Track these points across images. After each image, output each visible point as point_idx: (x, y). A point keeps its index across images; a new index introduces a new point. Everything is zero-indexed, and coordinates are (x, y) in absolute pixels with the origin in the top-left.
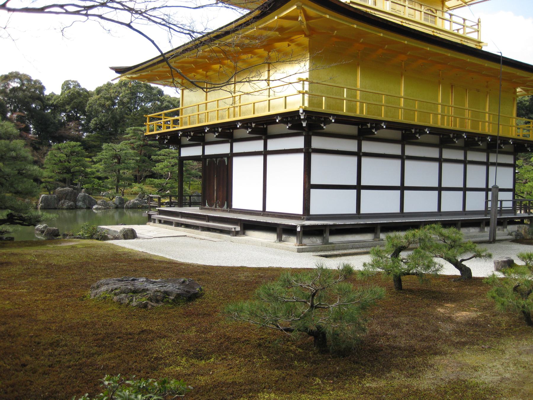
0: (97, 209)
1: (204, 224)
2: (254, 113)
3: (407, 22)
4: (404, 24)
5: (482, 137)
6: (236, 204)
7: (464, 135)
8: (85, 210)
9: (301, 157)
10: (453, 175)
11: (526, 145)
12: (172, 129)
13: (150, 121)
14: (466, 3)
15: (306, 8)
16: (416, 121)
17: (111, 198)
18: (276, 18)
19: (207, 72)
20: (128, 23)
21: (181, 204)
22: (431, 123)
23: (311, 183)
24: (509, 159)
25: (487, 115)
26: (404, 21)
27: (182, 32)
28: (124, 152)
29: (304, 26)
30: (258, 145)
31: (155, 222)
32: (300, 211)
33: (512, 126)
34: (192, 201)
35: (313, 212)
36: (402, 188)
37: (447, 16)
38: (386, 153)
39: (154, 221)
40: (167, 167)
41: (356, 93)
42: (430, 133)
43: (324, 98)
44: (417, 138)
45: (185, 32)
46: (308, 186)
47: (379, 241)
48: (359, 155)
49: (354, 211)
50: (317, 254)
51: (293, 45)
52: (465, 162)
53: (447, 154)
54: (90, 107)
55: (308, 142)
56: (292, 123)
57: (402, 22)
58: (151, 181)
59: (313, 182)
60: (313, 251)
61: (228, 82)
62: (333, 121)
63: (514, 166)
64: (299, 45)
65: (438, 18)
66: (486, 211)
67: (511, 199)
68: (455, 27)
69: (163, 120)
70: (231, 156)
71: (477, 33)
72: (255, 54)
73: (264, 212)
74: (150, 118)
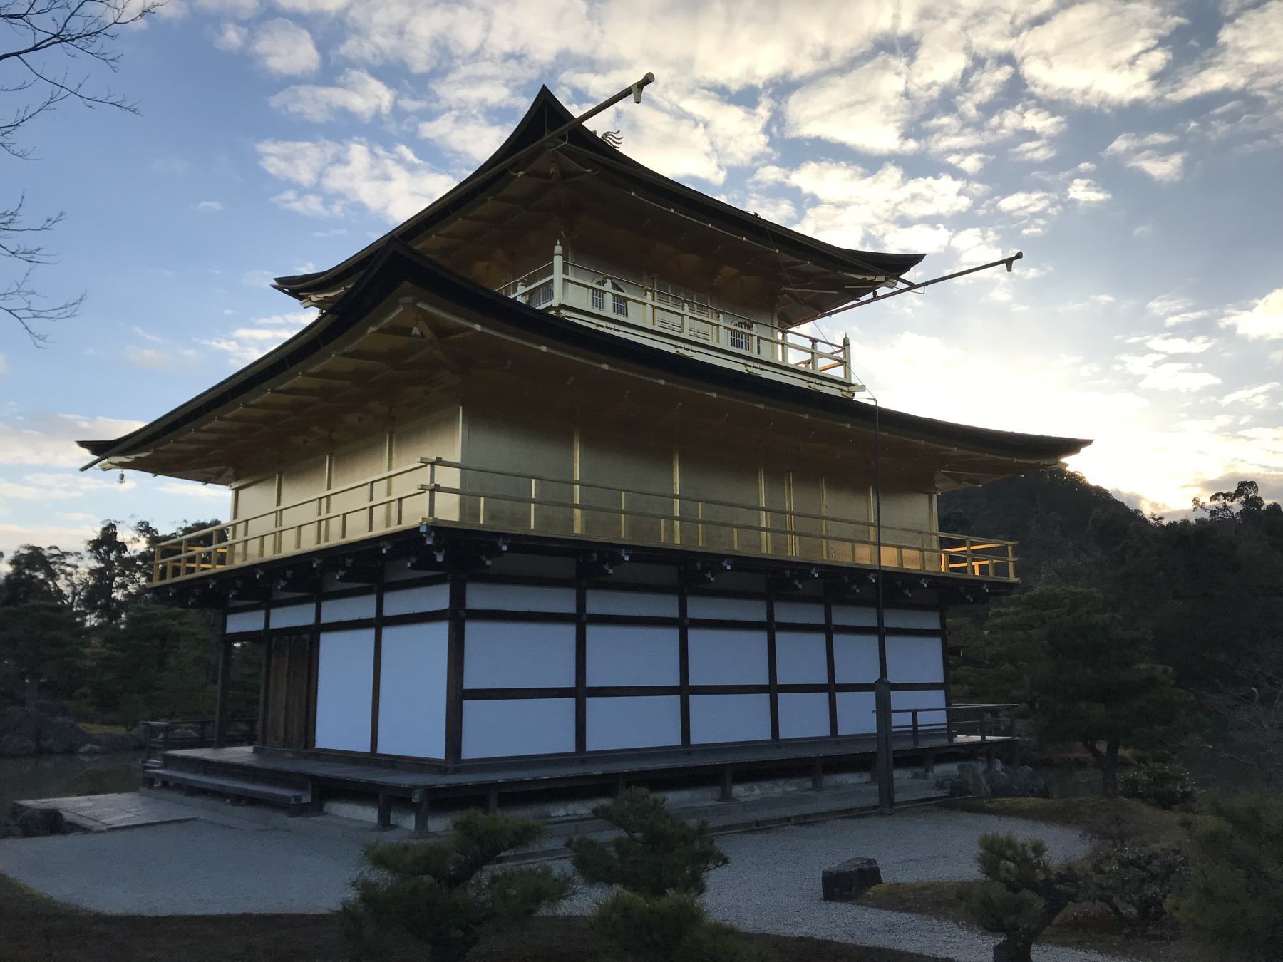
3: (688, 346)
4: (682, 351)
9: (441, 631)
10: (801, 657)
11: (962, 589)
13: (162, 557)
16: (701, 544)
23: (466, 687)
24: (933, 622)
30: (364, 607)
39: (149, 782)
46: (458, 695)
48: (581, 620)
49: (569, 746)
52: (828, 630)
53: (784, 613)
55: (458, 597)
59: (469, 684)
62: (505, 548)
70: (320, 628)
73: (373, 759)
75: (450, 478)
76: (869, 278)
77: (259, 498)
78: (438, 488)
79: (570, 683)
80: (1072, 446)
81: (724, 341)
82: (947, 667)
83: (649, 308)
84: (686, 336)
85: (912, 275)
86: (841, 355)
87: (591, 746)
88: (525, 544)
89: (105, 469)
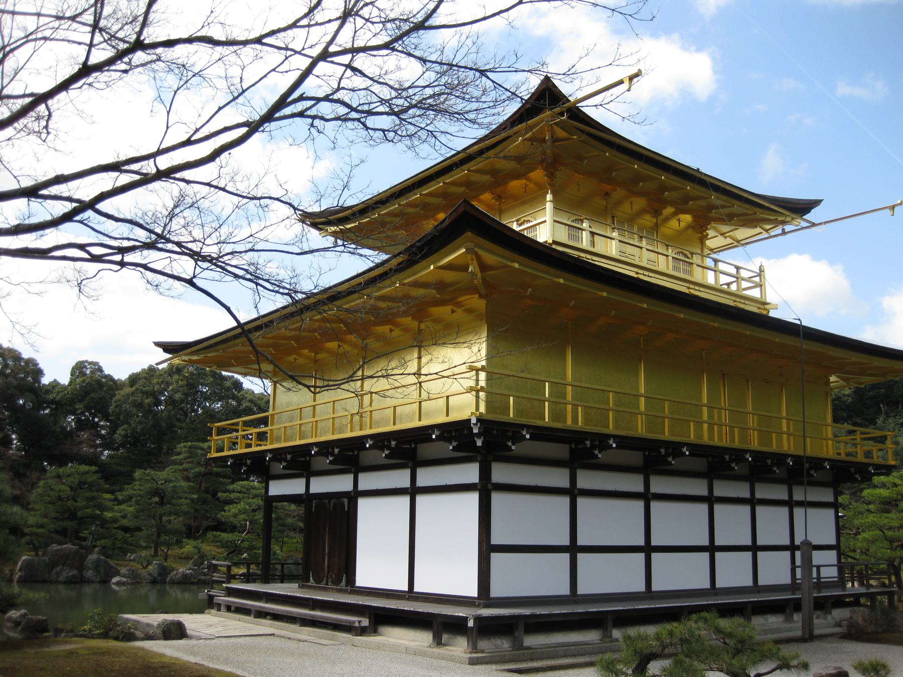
0: (118, 584)
1: (306, 615)
2: (394, 424)
4: (641, 277)
5: (779, 459)
7: (748, 456)
8: (98, 585)
9: (473, 498)
10: (733, 524)
11: (852, 470)
12: (254, 449)
14: (738, 241)
15: (480, 252)
16: (667, 436)
17: (145, 564)
18: (432, 267)
19: (316, 354)
20: (188, 277)
22: (692, 437)
24: (827, 495)
25: (784, 421)
27: (277, 292)
28: (171, 485)
29: (478, 281)
30: (400, 478)
31: (219, 610)
32: (471, 590)
33: (826, 439)
34: (286, 572)
35: (496, 591)
36: (648, 549)
37: (709, 263)
40: (244, 512)
41: (565, 389)
42: (690, 455)
43: (511, 398)
44: (670, 463)
45: (281, 290)
46: (487, 549)
47: (611, 642)
48: (573, 493)
49: (565, 590)
50: (503, 667)
51: (459, 311)
52: (752, 502)
53: (722, 489)
54: (116, 406)
55: (485, 473)
56: (458, 440)
57: (637, 273)
58: (215, 536)
59: (495, 540)
60: (496, 663)
61: (351, 376)
62: (528, 436)
63: (835, 506)
64: (470, 311)
65: (695, 266)
66: (794, 586)
67: (835, 562)
68: (724, 279)
69: (241, 433)
71: (758, 289)
72: (397, 325)
73: (411, 594)
74: (218, 428)
76: (780, 219)
79: (564, 540)
84: (644, 264)
85: (811, 216)
86: (757, 279)
87: (582, 590)
88: (542, 434)
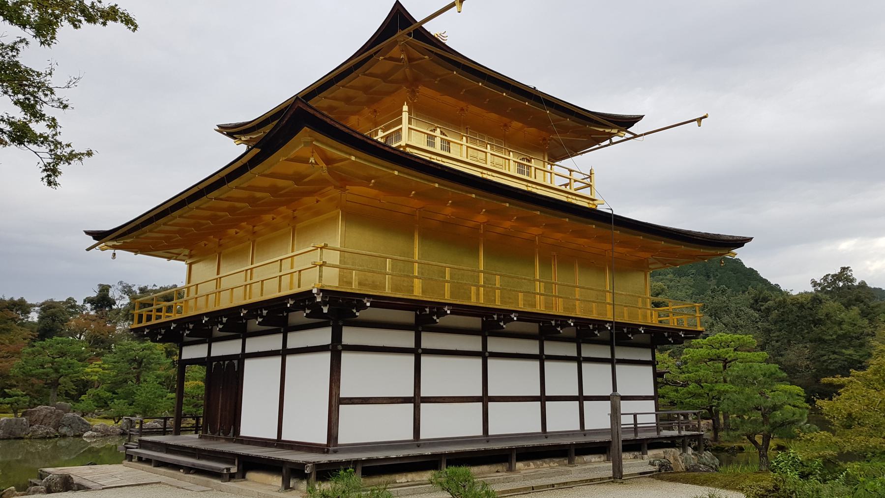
6: (246, 430)
9: (327, 357)
10: (561, 378)
11: (666, 334)
12: (163, 320)
13: (140, 308)
16: (498, 304)
21: (178, 431)
23: (341, 396)
26: (484, 172)
29: (325, 174)
30: (274, 342)
35: (343, 439)
38: (459, 349)
39: (130, 457)
46: (336, 401)
48: (417, 352)
49: (410, 436)
51: (322, 200)
52: (579, 360)
53: (551, 349)
55: (337, 336)
62: (368, 304)
63: (653, 363)
66: (611, 431)
70: (245, 355)
73: (279, 443)
75: (333, 257)
76: (607, 131)
77: (205, 270)
78: (324, 264)
79: (410, 393)
80: (740, 242)
81: (513, 171)
82: (656, 385)
83: (464, 148)
84: (488, 166)
89: (103, 250)
